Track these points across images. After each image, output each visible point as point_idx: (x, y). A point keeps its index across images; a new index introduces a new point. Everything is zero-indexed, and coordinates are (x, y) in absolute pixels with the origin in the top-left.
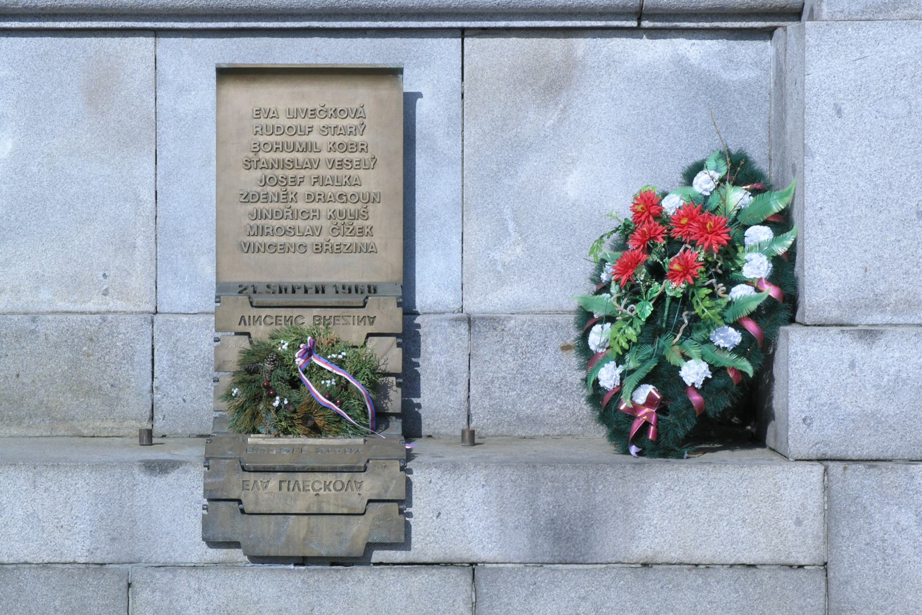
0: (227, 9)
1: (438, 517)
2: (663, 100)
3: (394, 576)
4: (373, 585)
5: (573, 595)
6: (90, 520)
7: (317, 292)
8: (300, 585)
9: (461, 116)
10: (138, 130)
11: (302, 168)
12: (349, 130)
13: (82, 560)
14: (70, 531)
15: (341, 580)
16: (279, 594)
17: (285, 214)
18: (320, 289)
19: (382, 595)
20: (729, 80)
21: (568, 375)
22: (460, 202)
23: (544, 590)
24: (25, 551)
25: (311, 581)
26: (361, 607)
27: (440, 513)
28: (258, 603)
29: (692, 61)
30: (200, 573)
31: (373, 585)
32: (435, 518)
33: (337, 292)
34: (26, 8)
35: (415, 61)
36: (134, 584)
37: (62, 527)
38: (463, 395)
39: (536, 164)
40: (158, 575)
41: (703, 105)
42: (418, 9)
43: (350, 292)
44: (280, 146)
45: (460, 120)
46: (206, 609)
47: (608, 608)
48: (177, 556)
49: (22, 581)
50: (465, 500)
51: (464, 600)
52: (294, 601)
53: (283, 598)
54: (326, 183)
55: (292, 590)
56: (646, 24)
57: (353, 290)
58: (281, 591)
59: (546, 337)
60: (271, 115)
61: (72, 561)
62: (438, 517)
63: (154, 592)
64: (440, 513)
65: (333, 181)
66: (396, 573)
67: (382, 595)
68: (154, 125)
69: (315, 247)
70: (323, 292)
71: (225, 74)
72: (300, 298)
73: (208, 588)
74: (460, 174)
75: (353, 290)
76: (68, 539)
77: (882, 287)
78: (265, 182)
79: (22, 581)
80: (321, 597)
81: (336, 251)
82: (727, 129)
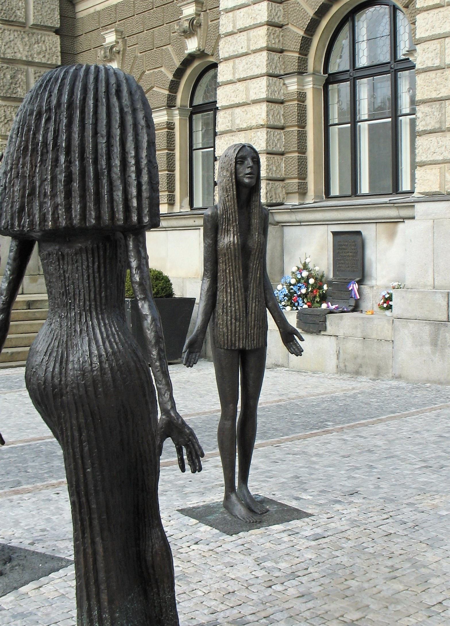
71: (335, 234)
77: (419, 281)
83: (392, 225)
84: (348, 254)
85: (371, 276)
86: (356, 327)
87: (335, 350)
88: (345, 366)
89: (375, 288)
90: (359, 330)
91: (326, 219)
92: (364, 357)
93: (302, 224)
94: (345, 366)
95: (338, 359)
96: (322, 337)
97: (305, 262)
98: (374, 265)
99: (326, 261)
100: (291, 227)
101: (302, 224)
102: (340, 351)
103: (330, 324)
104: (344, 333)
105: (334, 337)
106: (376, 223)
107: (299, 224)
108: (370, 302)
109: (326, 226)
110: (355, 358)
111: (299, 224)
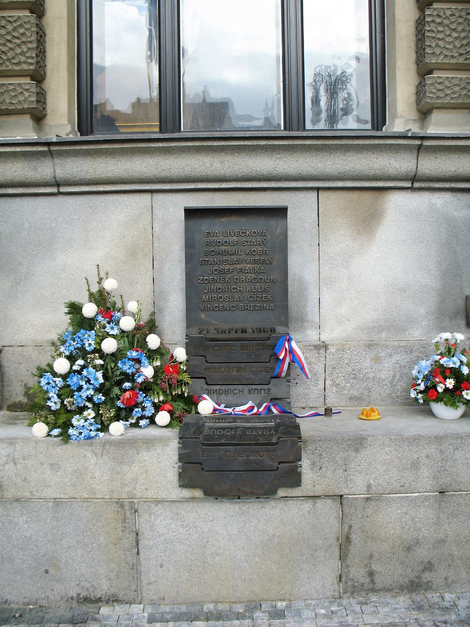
0: (190, 177)
1: (320, 469)
2: (424, 227)
3: (294, 504)
4: (281, 510)
5: (399, 512)
6: (111, 474)
7: (242, 332)
8: (237, 510)
9: (318, 235)
10: (143, 245)
11: (233, 264)
12: (258, 243)
13: (107, 497)
14: (99, 480)
15: (262, 507)
16: (225, 516)
17: (224, 289)
18: (244, 331)
19: (287, 515)
20: (458, 216)
21: (378, 374)
22: (318, 281)
23: (382, 509)
24: (74, 492)
25: (244, 508)
26: (274, 522)
27: (321, 467)
28: (212, 521)
29: (438, 206)
30: (178, 504)
31: (281, 510)
32: (318, 470)
33: (253, 332)
34: (81, 179)
35: (292, 206)
36: (139, 510)
37: (95, 478)
38: (322, 386)
39: (358, 261)
40: (153, 506)
41: (444, 229)
42: (295, 177)
43: (260, 332)
44: (220, 252)
45: (317, 238)
46: (182, 525)
47: (419, 518)
48: (163, 495)
49: (73, 509)
50: (337, 459)
51: (335, 516)
52: (234, 520)
53: (228, 518)
54: (246, 271)
55: (233, 513)
56: (416, 185)
57: (262, 330)
58: (226, 514)
59: (366, 354)
60: (215, 235)
61: (101, 497)
62: (320, 469)
63: (150, 515)
64: (321, 467)
65: (250, 271)
66: (295, 502)
67: (287, 515)
68: (151, 242)
69: (240, 307)
70: (246, 332)
72: (233, 335)
73: (183, 513)
74: (318, 266)
75: (262, 330)
76: (98, 485)
78: (213, 272)
79: (73, 509)
80: (250, 517)
81: (252, 309)
82: (457, 242)
83: (368, 196)
84: (239, 266)
85: (302, 320)
86: (415, 465)
87: (333, 536)
88: (371, 574)
89: (332, 349)
90: (425, 472)
91: (165, 174)
92: (441, 542)
93: (62, 189)
94: (371, 574)
95: (343, 557)
96: (281, 505)
97: (101, 292)
98: (313, 293)
99: (149, 286)
100: (18, 201)
101: (62, 189)
102: (353, 536)
103: (313, 464)
104: (369, 487)
105: (329, 501)
106: (318, 189)
107: (54, 190)
108: (316, 384)
109: (147, 197)
110: (409, 549)
111: (54, 190)
